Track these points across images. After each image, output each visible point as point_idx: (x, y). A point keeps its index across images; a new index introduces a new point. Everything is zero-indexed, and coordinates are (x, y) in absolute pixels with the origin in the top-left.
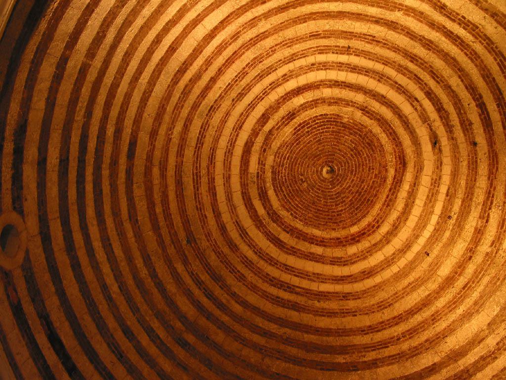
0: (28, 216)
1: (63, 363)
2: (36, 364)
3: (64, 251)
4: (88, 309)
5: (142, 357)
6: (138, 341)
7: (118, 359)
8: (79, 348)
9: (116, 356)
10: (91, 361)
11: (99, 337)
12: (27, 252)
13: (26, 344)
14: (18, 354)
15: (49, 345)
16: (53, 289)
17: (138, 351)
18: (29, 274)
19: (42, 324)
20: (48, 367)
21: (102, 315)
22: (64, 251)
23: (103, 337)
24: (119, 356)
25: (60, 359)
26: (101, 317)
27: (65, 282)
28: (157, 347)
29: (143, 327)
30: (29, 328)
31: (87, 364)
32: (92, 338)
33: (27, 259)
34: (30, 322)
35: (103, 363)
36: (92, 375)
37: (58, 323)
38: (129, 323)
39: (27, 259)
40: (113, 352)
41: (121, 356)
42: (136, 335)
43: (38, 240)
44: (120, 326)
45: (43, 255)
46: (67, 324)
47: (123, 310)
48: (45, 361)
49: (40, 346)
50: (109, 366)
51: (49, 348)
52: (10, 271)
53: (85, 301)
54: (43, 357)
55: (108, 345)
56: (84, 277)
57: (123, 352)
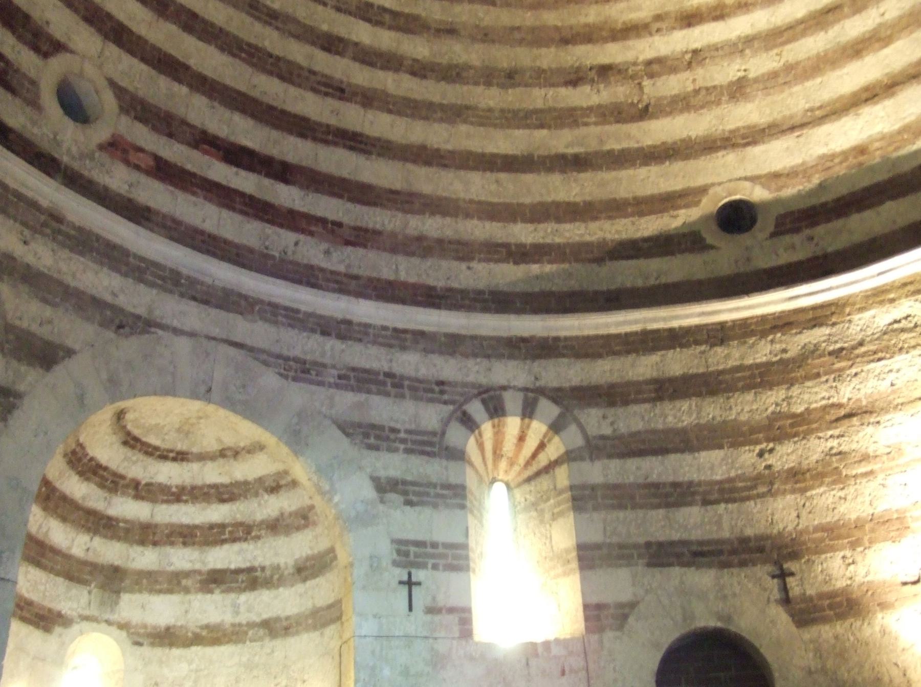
0: (69, 39)
1: (268, 175)
2: (233, 209)
3: (158, 21)
4: (253, 65)
5: (372, 64)
6: (356, 44)
7: (341, 99)
8: (275, 134)
9: (333, 96)
10: (302, 135)
11: (293, 91)
12: (112, 84)
13: (205, 198)
14: (204, 221)
15: (234, 169)
16: (184, 90)
17: (363, 62)
18: (139, 108)
19: (205, 152)
20: (251, 197)
21: (278, 53)
22: (158, 21)
23: (300, 86)
24: (338, 94)
25: (259, 173)
26: (278, 59)
27: (192, 62)
28: (390, 28)
29: (350, 14)
30: (194, 175)
31: (300, 145)
32: (284, 101)
33: (119, 91)
34: (189, 167)
35: (320, 124)
36: (317, 154)
37: (225, 127)
38: (325, 27)
39: (119, 91)
40: (326, 94)
41: (342, 91)
42: (346, 36)
43: (113, 50)
44: (313, 43)
45: (135, 62)
46: (237, 117)
47: (304, 15)
48: (242, 195)
49: (224, 183)
50: (333, 121)
51: (237, 174)
52: (113, 136)
53: (240, 58)
54: (236, 192)
55: (314, 90)
56: (212, 25)
57: (342, 82)
